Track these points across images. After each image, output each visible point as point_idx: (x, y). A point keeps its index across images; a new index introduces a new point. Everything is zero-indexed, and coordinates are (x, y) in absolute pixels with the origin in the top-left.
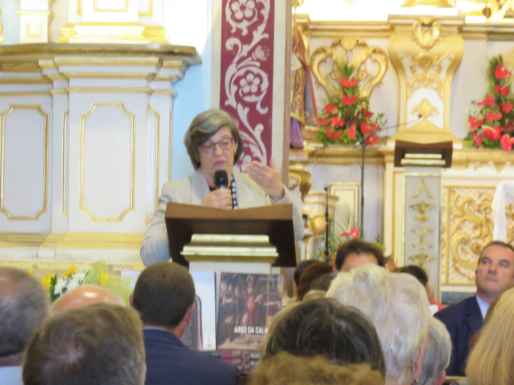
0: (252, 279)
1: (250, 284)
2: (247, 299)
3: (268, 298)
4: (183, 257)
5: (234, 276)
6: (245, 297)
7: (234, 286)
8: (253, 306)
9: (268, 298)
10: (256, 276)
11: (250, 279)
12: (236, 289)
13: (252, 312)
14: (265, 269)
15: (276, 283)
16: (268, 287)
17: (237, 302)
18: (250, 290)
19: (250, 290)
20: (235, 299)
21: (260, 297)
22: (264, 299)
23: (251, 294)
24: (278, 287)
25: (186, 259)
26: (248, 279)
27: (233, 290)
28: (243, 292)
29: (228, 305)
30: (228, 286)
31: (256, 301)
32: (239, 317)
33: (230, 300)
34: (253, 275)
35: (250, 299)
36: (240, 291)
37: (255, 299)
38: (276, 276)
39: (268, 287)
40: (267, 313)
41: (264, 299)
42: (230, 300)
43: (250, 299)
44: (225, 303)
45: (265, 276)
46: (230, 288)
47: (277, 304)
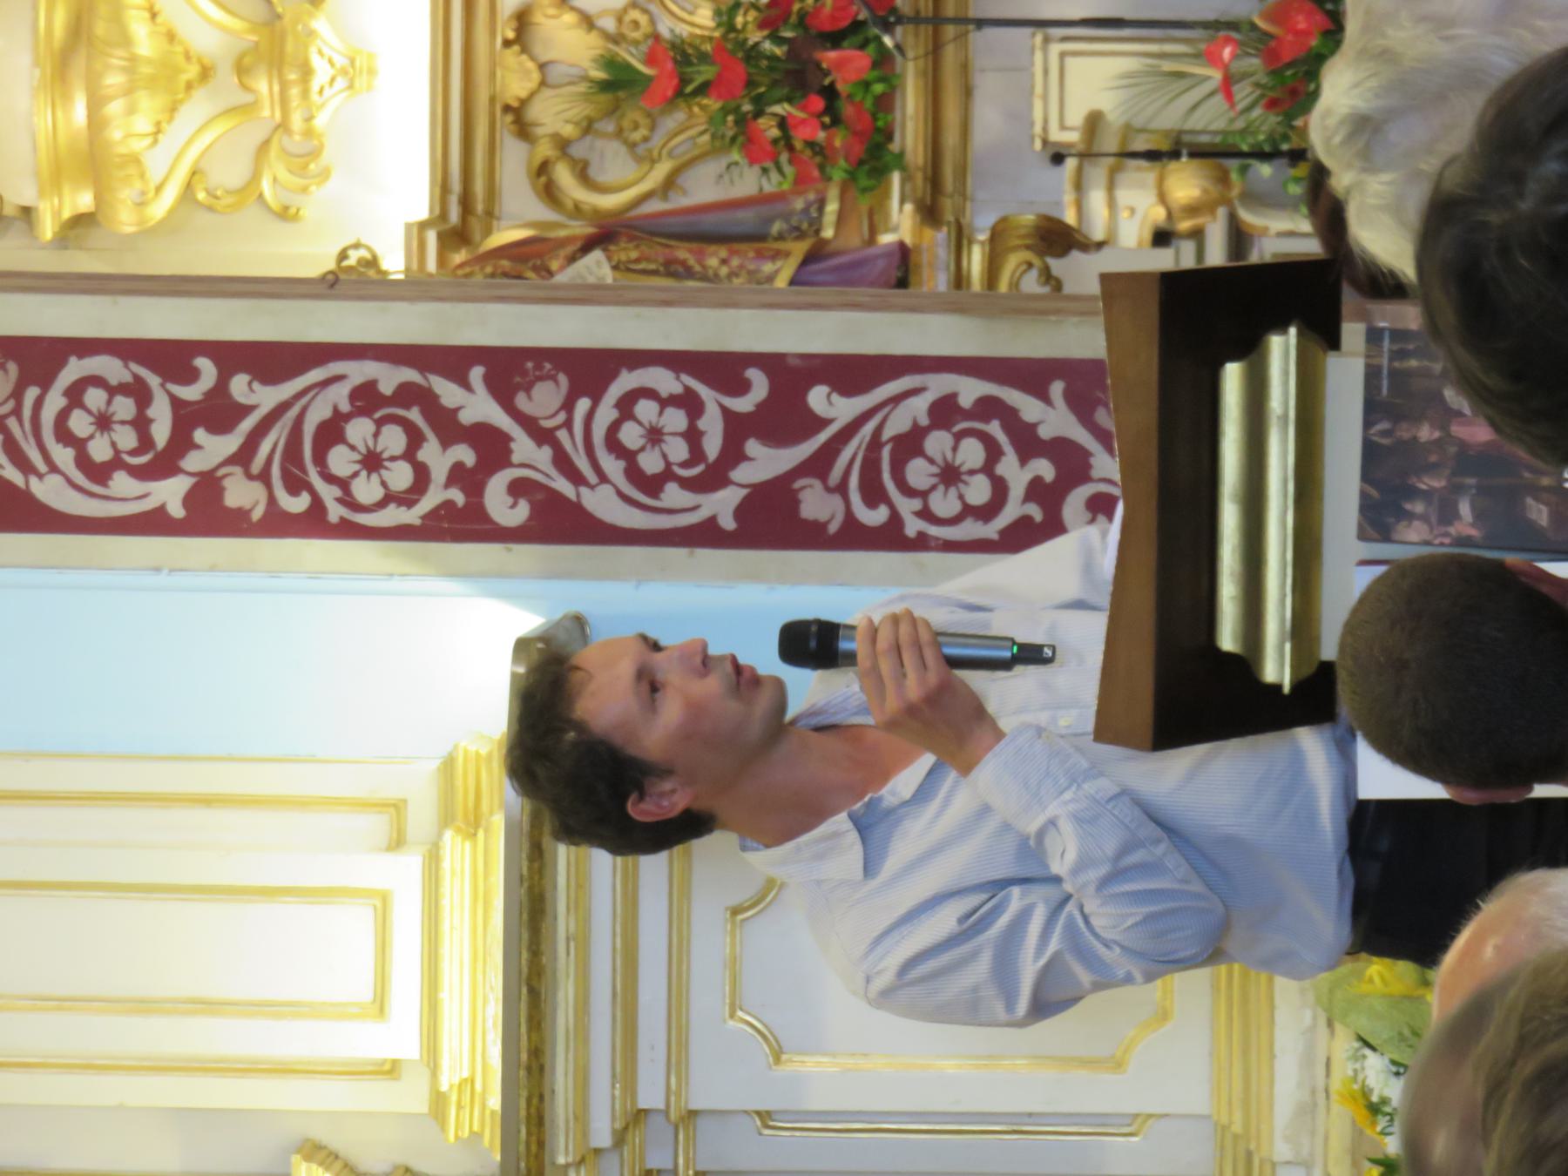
0: (1383, 426)
1: (1404, 432)
2: (1463, 445)
4: (1296, 686)
5: (1374, 493)
6: (1453, 450)
7: (1413, 493)
10: (1373, 408)
11: (1385, 433)
12: (1424, 487)
14: (1346, 375)
15: (1398, 335)
16: (1413, 363)
17: (1471, 481)
18: (1426, 433)
19: (1426, 433)
20: (1456, 489)
23: (1444, 428)
25: (1308, 671)
26: (1385, 441)
27: (1427, 495)
28: (1433, 458)
29: (1479, 516)
30: (1410, 516)
31: (1467, 410)
32: (1527, 475)
33: (1465, 508)
34: (1368, 424)
35: (1457, 430)
36: (1431, 469)
37: (1459, 414)
38: (1374, 336)
39: (1413, 363)
42: (1465, 508)
43: (1457, 430)
44: (1473, 525)
45: (1372, 376)
46: (1418, 507)
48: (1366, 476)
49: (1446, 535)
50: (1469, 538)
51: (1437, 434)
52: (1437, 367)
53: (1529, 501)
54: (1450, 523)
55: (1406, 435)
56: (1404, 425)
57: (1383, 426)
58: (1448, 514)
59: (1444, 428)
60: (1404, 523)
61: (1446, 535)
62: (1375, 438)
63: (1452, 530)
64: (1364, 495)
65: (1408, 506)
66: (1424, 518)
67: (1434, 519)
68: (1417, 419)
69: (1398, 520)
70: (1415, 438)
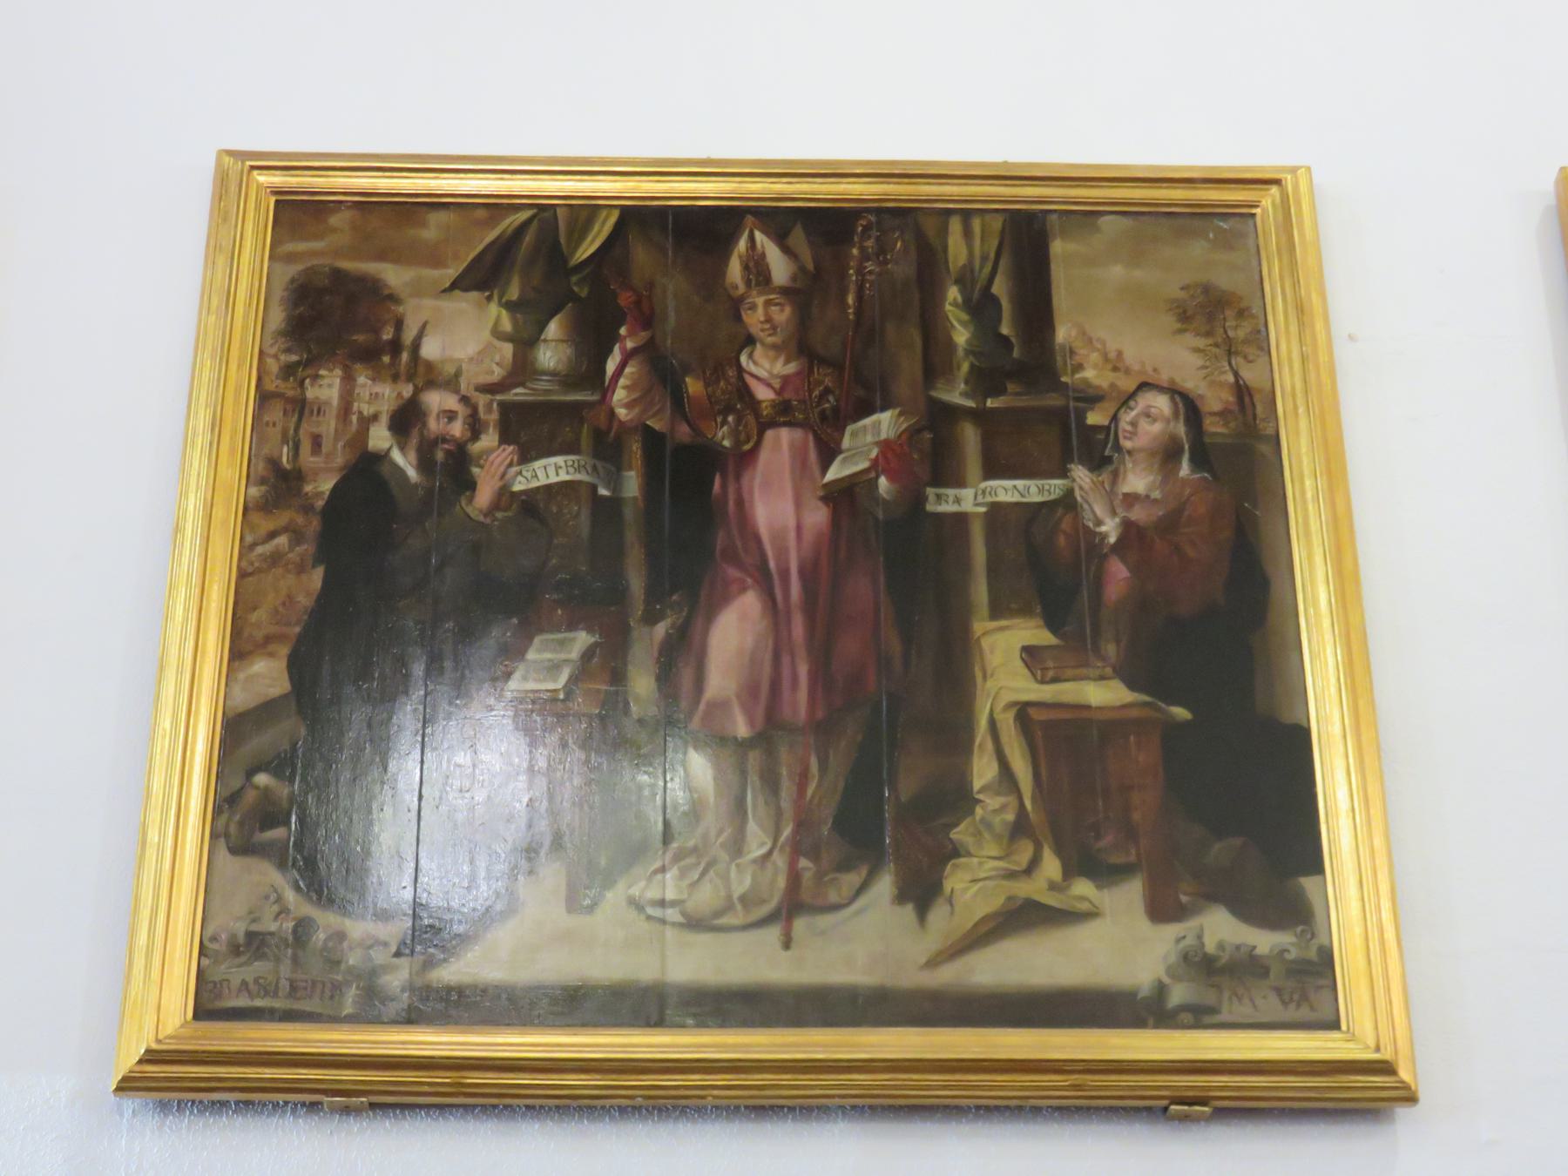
0: (780, 268)
2: (746, 458)
3: (970, 437)
7: (593, 340)
8: (817, 516)
9: (970, 437)
11: (757, 271)
12: (611, 366)
13: (809, 574)
17: (632, 484)
20: (607, 447)
21: (885, 423)
22: (931, 452)
24: (1063, 333)
26: (734, 270)
27: (588, 372)
29: (531, 508)
30: (525, 342)
31: (833, 474)
33: (551, 470)
35: (781, 447)
36: (663, 373)
37: (828, 453)
40: (980, 591)
41: (931, 452)
42: (551, 470)
44: (505, 496)
47: (1068, 502)
48: (638, 219)
49: (475, 428)
50: (471, 485)
51: (763, 394)
52: (956, 394)
53: (582, 639)
54: (505, 439)
55: (754, 319)
56: (783, 315)
57: (780, 268)
58: (530, 428)
59: (784, 413)
60: (507, 325)
61: (475, 428)
62: (742, 244)
63: (489, 439)
64: (584, 212)
65: (553, 329)
66: (522, 369)
67: (518, 394)
68: (802, 346)
69: (511, 306)
70: (750, 341)
